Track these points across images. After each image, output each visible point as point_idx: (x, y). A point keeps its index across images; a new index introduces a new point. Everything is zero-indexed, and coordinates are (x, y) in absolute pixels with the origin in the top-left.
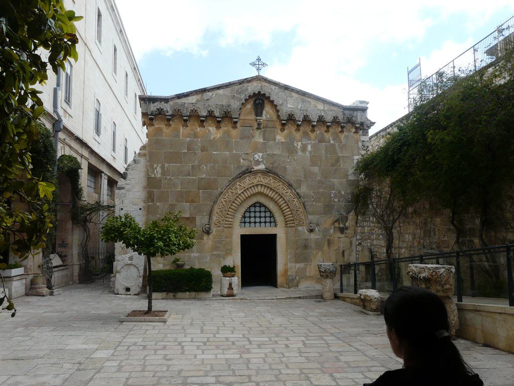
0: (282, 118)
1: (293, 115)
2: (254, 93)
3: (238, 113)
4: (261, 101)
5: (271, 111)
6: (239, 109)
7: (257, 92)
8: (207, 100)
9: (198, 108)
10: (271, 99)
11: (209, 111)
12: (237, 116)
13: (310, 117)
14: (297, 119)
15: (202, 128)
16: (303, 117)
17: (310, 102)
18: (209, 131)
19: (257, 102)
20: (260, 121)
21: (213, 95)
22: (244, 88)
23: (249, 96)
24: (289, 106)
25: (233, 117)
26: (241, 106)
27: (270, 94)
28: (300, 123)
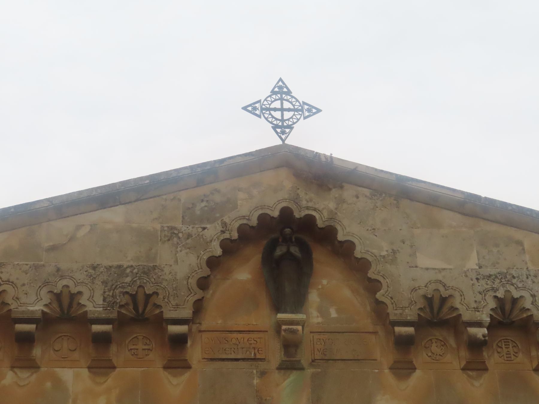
0: (393, 314)
1: (444, 300)
2: (263, 218)
3: (192, 299)
4: (295, 250)
5: (347, 293)
6: (193, 282)
7: (276, 214)
8: (53, 248)
9: (8, 282)
10: (341, 237)
11: (58, 297)
12: (186, 313)
13: (528, 304)
14: (466, 316)
15: (24, 374)
16: (492, 304)
17: (520, 243)
18: (58, 383)
19: (279, 251)
20: (294, 332)
21: (79, 227)
22: (218, 198)
23: (241, 229)
24: (423, 261)
25: (169, 314)
26: (206, 271)
27: (333, 216)
28: (480, 332)
